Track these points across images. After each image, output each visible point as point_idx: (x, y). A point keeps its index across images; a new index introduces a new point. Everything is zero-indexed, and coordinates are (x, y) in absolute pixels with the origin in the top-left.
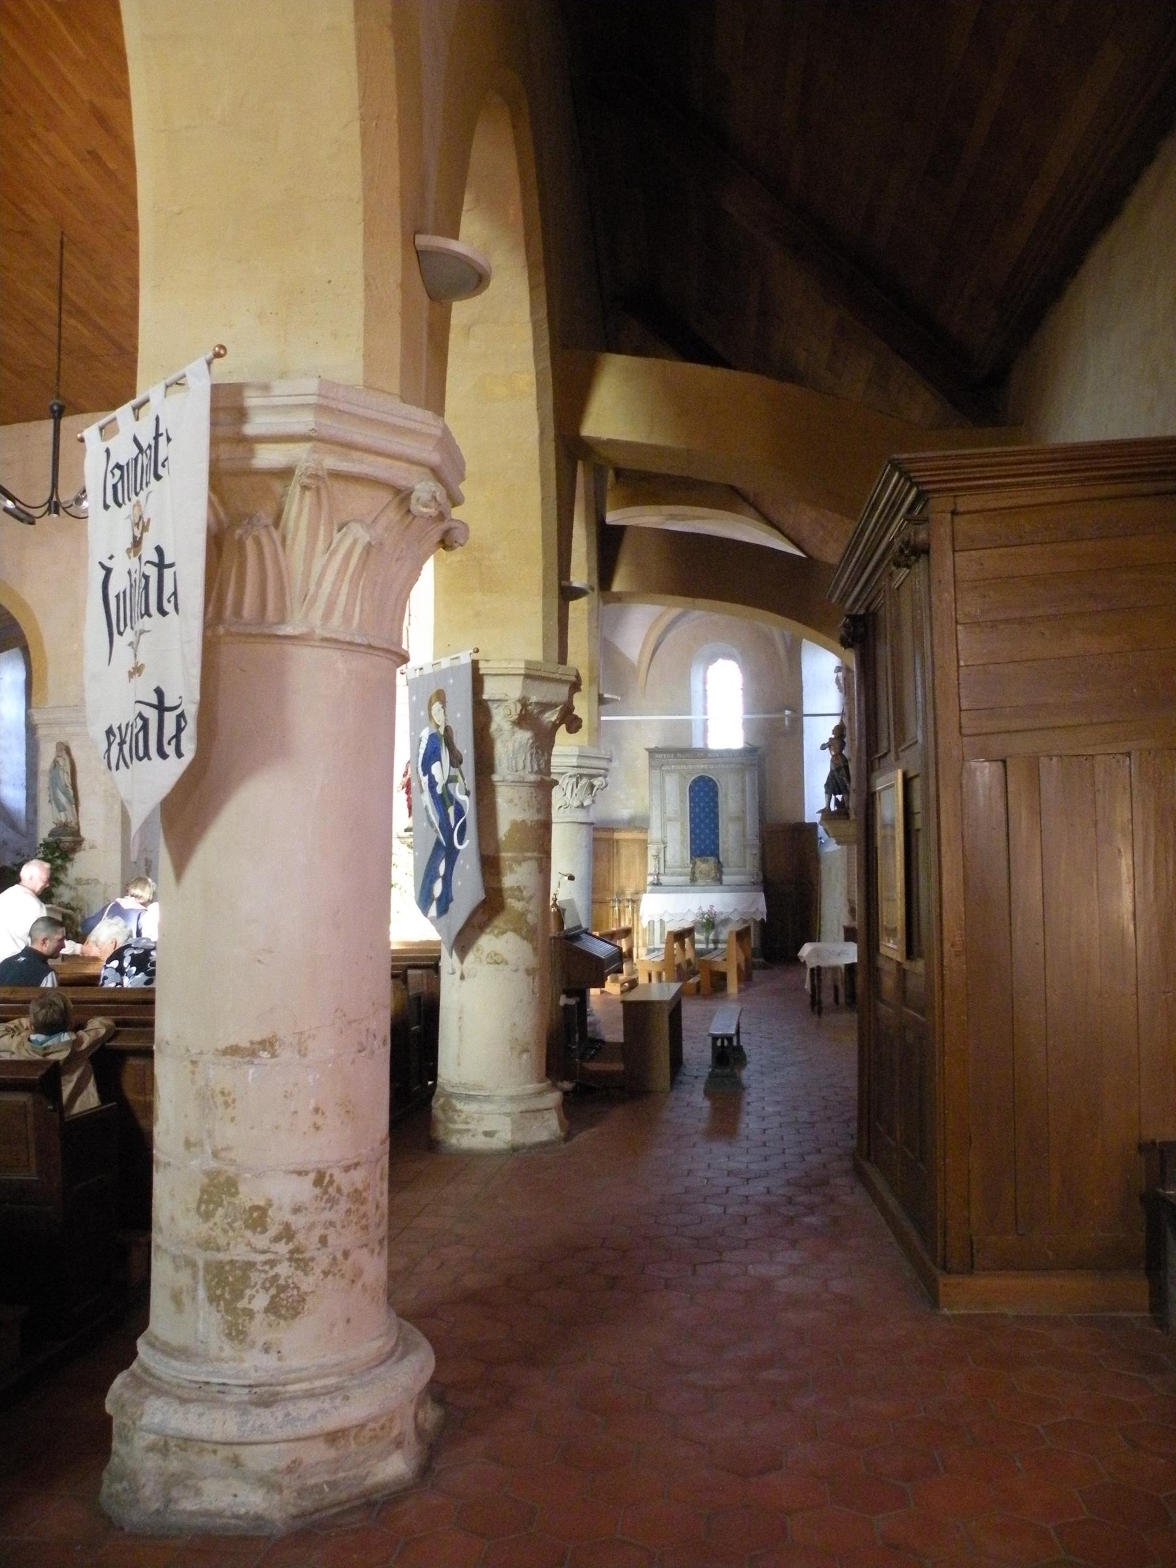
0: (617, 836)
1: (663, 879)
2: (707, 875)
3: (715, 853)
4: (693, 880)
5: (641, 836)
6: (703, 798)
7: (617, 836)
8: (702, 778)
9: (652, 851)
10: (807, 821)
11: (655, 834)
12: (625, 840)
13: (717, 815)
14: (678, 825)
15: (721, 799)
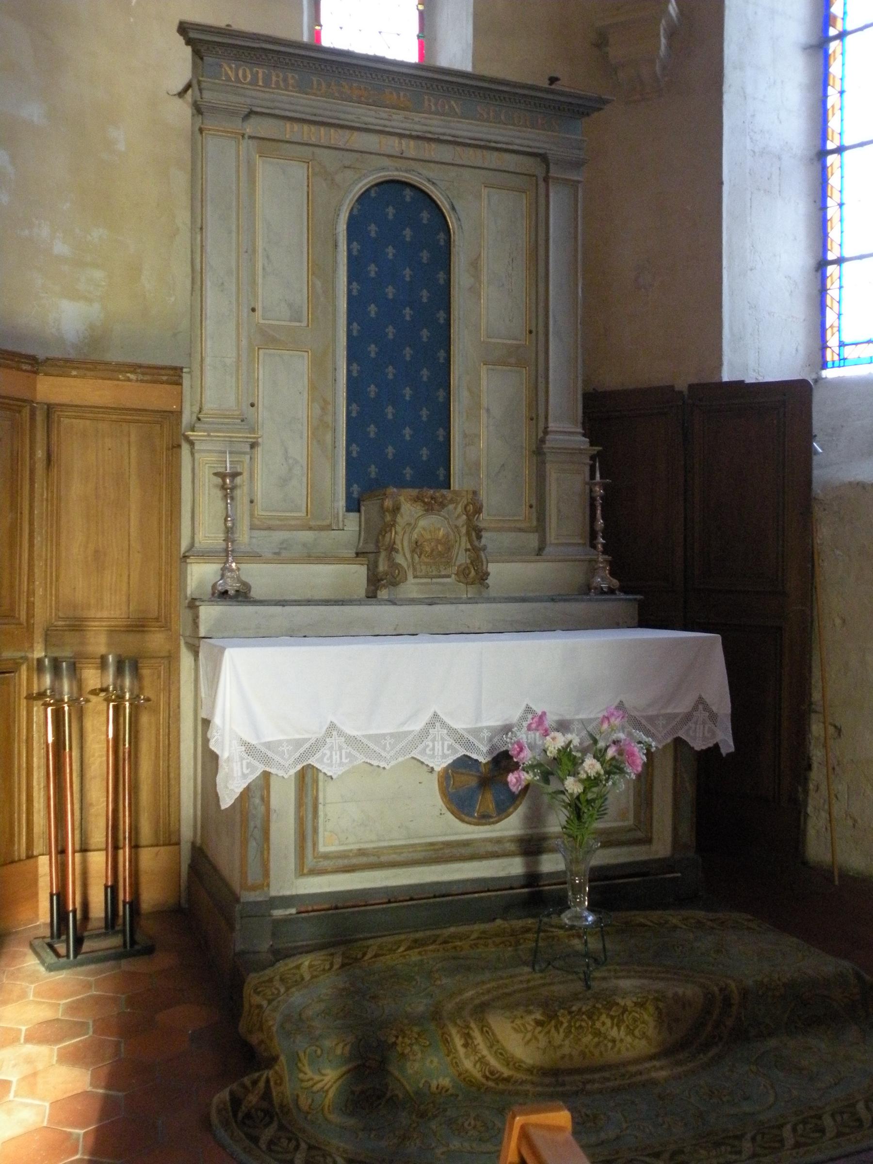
0: (49, 389)
1: (260, 576)
2: (438, 555)
3: (432, 473)
4: (378, 585)
5: (155, 397)
6: (397, 255)
7: (49, 389)
8: (392, 187)
9: (199, 470)
10: (726, 377)
11: (213, 389)
12: (81, 410)
13: (443, 337)
14: (302, 364)
15: (461, 277)
